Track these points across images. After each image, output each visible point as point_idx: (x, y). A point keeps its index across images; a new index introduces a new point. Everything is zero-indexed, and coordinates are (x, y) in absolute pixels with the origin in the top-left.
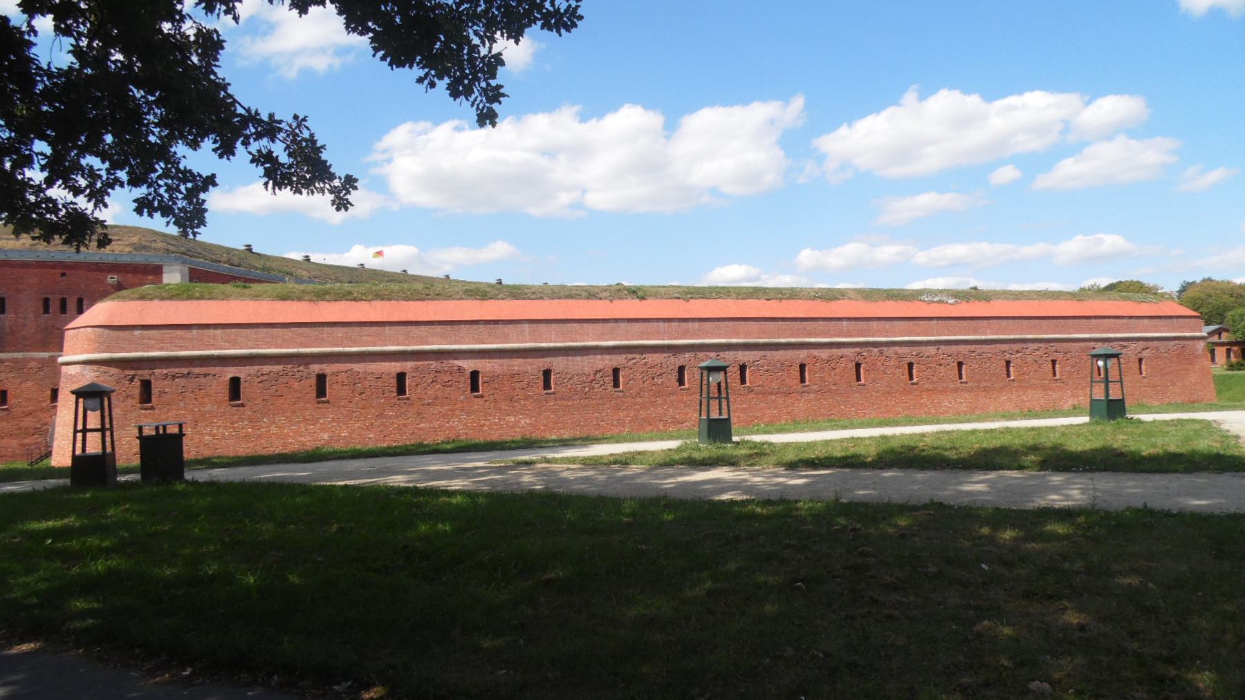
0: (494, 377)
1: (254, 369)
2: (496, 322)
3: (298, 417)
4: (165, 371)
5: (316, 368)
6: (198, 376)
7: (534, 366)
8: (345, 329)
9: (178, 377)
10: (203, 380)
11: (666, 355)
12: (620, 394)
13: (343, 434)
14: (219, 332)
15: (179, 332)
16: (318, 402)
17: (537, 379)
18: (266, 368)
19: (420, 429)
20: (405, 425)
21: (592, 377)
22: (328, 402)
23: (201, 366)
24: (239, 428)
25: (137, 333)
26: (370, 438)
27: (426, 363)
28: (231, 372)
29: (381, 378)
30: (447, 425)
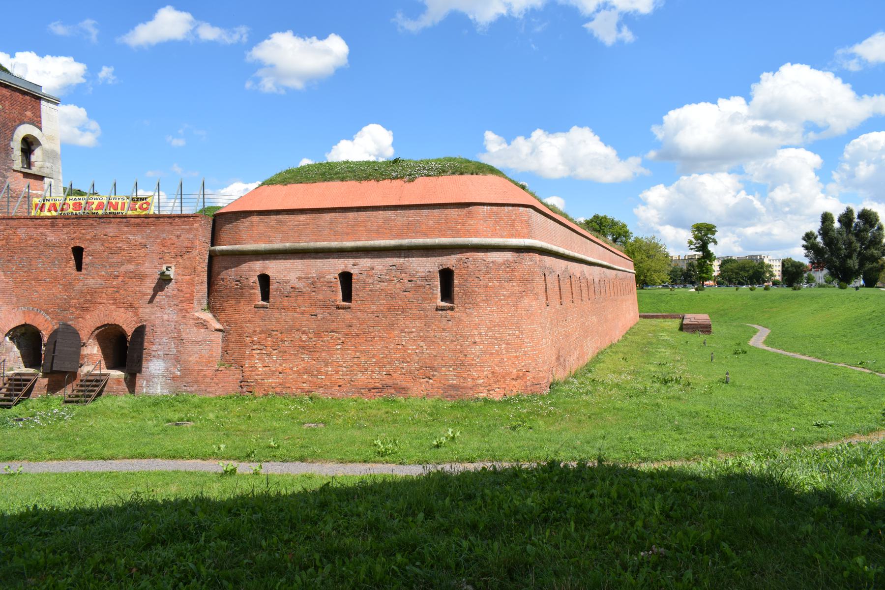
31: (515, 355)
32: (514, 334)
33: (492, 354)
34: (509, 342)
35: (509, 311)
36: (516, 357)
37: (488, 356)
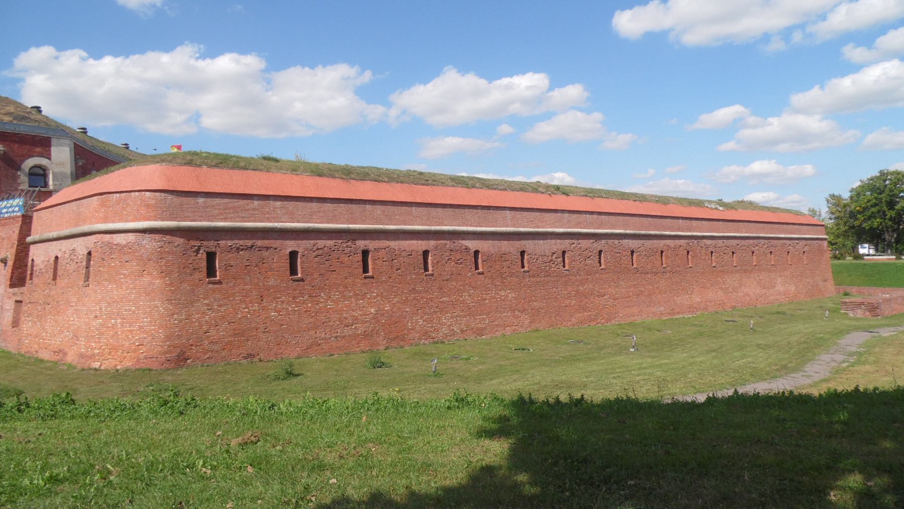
0: (489, 258)
1: (310, 243)
2: (488, 208)
3: (349, 292)
4: (230, 243)
5: (362, 244)
6: (260, 249)
7: (511, 247)
8: (383, 208)
9: (242, 250)
10: (265, 254)
11: (591, 241)
12: (567, 272)
13: (386, 308)
14: (279, 204)
15: (242, 202)
16: (365, 278)
17: (517, 259)
18: (321, 243)
19: (442, 302)
20: (431, 300)
21: (550, 258)
22: (372, 277)
23: (264, 239)
24: (301, 303)
25: (201, 200)
26: (407, 312)
27: (443, 242)
28: (291, 245)
29: (411, 255)
30: (461, 299)
31: (129, 329)
32: (130, 310)
33: (109, 327)
34: (125, 317)
35: (127, 289)
36: (130, 331)
37: (105, 329)
